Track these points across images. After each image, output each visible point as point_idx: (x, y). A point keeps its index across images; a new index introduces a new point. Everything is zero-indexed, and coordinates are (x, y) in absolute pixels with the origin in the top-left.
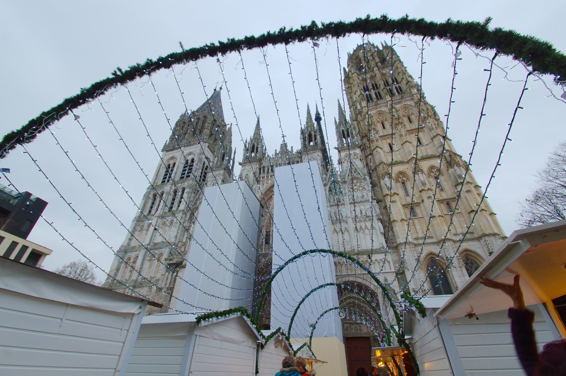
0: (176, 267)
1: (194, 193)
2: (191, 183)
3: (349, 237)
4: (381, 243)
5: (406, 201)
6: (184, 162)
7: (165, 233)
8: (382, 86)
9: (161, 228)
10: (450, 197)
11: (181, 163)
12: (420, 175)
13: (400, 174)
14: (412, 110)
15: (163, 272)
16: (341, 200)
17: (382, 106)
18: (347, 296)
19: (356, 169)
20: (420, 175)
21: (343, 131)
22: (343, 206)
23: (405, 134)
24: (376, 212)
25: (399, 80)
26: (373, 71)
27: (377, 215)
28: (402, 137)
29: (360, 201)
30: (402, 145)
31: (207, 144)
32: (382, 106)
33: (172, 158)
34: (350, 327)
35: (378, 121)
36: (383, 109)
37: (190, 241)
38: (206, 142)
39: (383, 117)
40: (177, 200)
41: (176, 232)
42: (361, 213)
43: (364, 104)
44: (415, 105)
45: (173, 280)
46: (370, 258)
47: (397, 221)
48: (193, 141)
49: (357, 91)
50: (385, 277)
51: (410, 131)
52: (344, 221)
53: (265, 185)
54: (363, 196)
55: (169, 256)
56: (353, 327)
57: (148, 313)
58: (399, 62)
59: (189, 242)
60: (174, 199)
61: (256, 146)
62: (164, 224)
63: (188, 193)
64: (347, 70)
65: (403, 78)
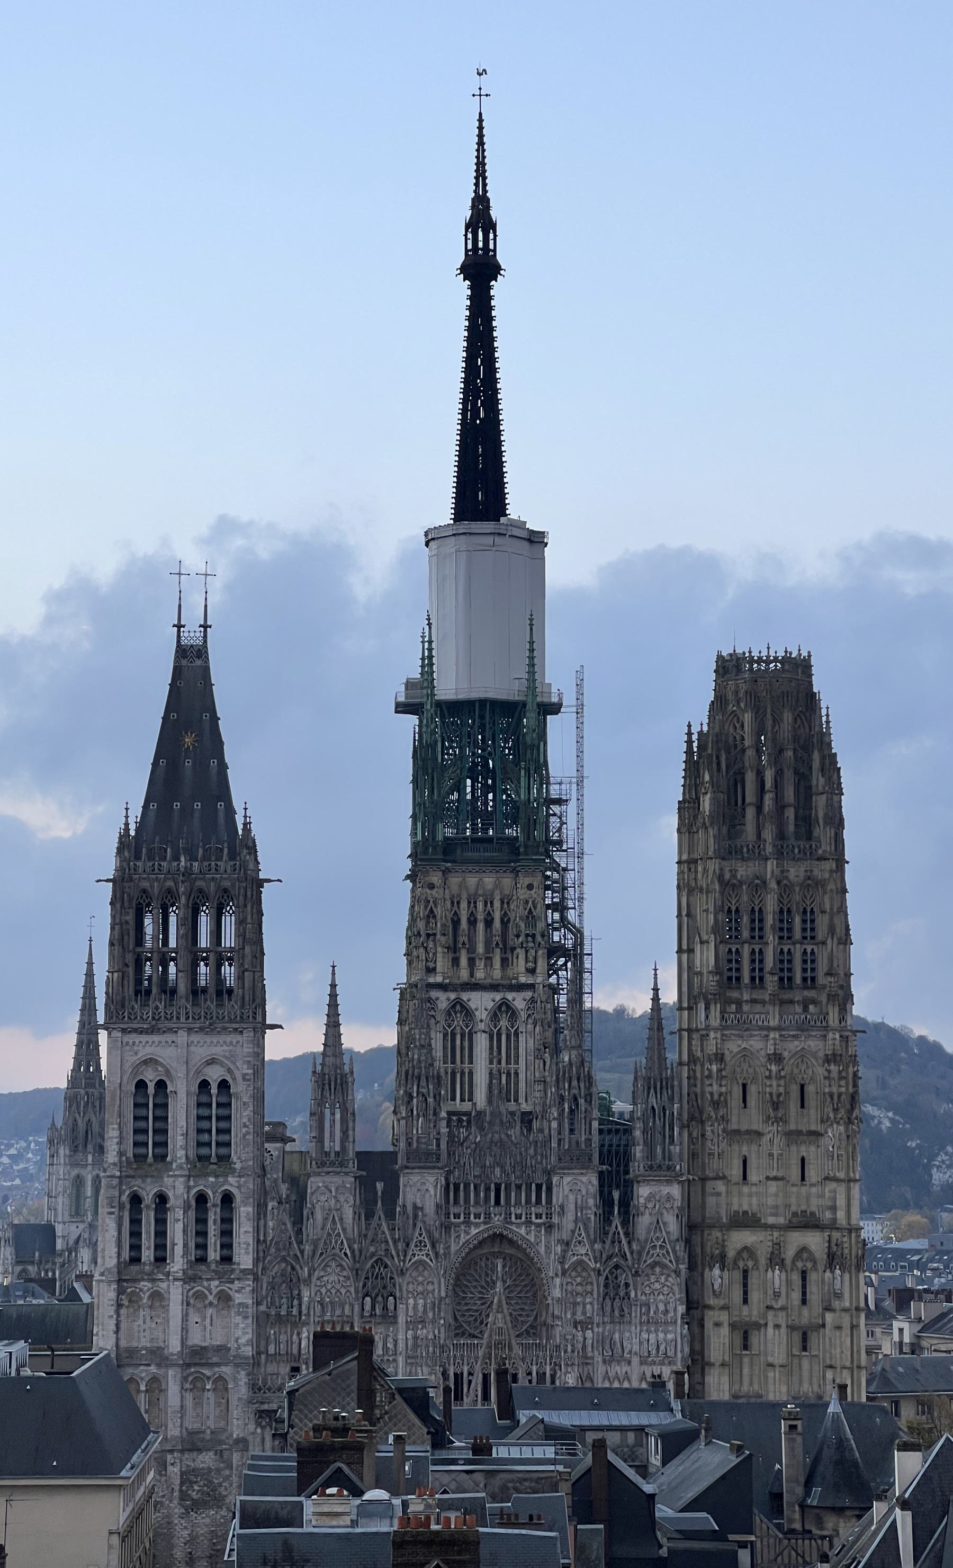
6: (195, 1088)
9: (194, 1306)
12: (777, 1272)
15: (251, 1427)
17: (755, 1035)
19: (664, 1242)
20: (777, 1272)
24: (682, 1351)
32: (755, 1035)
33: (149, 1062)
39: (750, 1066)
47: (713, 1365)
51: (793, 1136)
54: (666, 1312)
60: (201, 1221)
62: (199, 1296)
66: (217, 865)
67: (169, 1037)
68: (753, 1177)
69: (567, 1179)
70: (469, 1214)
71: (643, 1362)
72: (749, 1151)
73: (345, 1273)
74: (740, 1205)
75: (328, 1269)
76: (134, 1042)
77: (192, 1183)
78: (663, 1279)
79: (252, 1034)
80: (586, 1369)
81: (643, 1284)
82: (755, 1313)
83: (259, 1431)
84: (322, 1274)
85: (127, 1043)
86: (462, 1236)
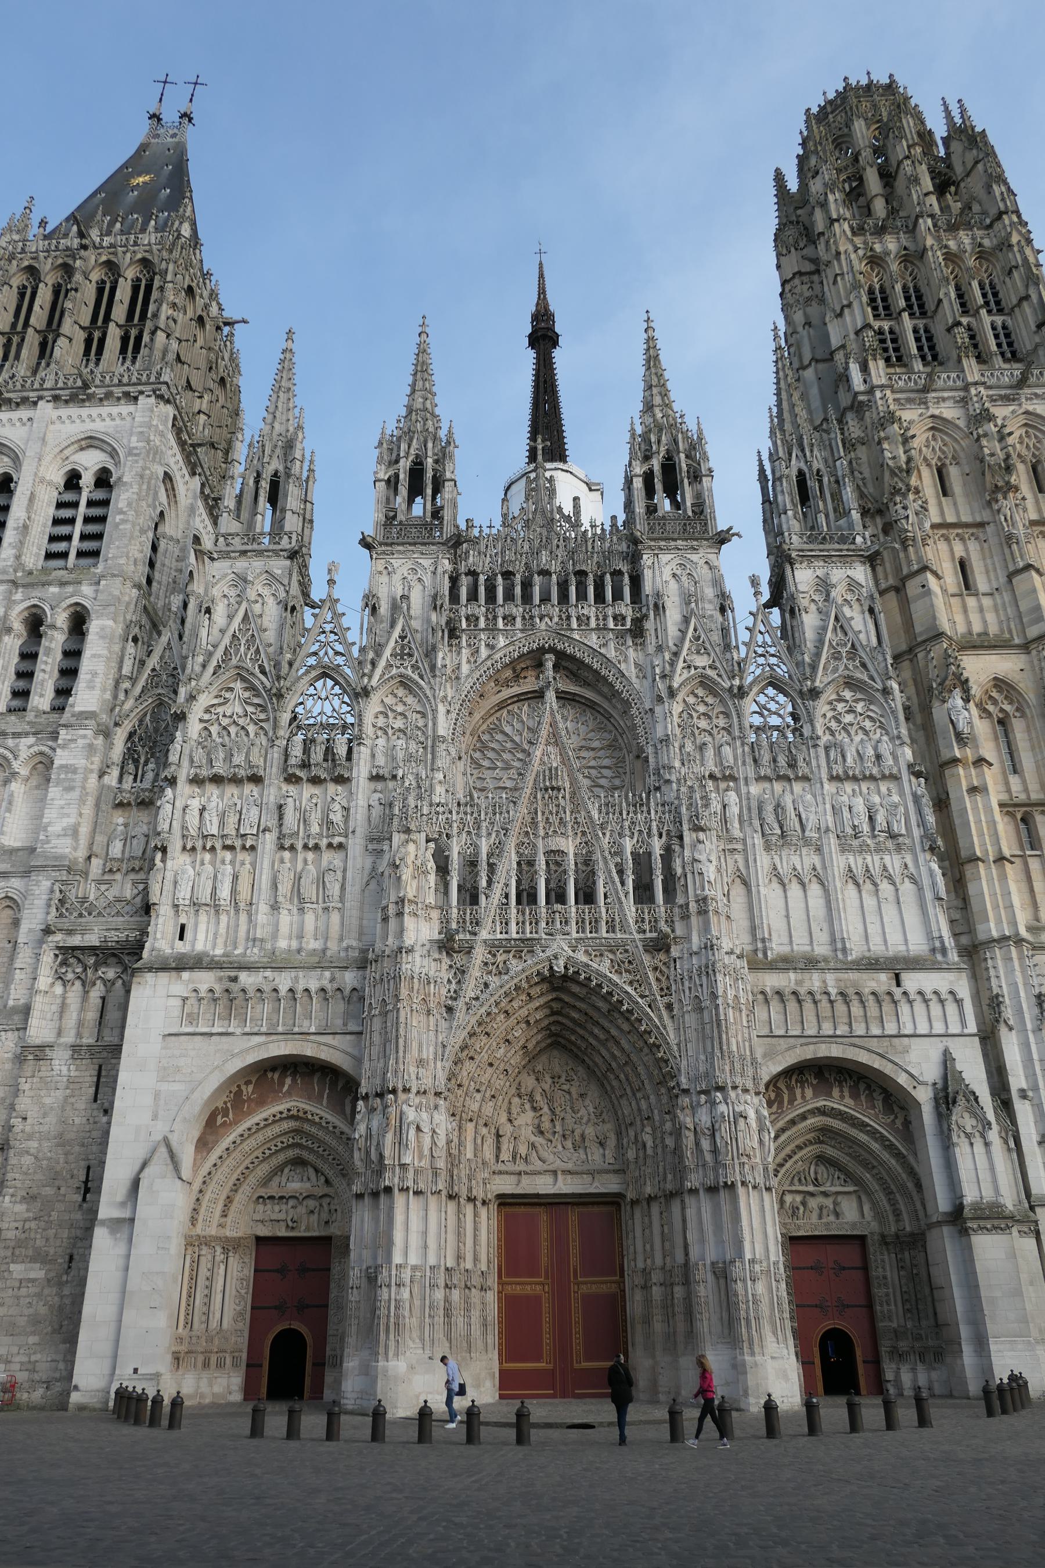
1: (135, 640)
2: (117, 593)
3: (821, 902)
5: (1009, 791)
7: (9, 810)
11: (42, 481)
13: (995, 686)
16: (801, 763)
17: (944, 399)
18: (809, 1107)
21: (801, 474)
22: (806, 785)
24: (922, 823)
25: (1009, 297)
26: (912, 229)
28: (1015, 547)
29: (868, 773)
30: (1010, 576)
31: (170, 410)
32: (944, 399)
34: (804, 1203)
35: (925, 459)
36: (949, 412)
37: (163, 861)
38: (168, 401)
40: (50, 661)
41: (73, 811)
42: (870, 818)
43: (879, 371)
45: (92, 1015)
46: (898, 985)
49: (849, 305)
52: (807, 842)
53: (484, 652)
54: (878, 757)
55: (61, 915)
56: (813, 1203)
58: (1015, 219)
60: (29, 656)
61: (429, 474)
64: (793, 184)
65: (1027, 297)
67: (24, 413)
68: (982, 583)
69: (665, 558)
70: (495, 618)
71: (844, 849)
72: (967, 550)
73: (256, 701)
74: (969, 623)
75: (227, 695)
77: (18, 596)
79: (152, 400)
80: (731, 862)
82: (1034, 786)
83: (58, 989)
84: (216, 701)
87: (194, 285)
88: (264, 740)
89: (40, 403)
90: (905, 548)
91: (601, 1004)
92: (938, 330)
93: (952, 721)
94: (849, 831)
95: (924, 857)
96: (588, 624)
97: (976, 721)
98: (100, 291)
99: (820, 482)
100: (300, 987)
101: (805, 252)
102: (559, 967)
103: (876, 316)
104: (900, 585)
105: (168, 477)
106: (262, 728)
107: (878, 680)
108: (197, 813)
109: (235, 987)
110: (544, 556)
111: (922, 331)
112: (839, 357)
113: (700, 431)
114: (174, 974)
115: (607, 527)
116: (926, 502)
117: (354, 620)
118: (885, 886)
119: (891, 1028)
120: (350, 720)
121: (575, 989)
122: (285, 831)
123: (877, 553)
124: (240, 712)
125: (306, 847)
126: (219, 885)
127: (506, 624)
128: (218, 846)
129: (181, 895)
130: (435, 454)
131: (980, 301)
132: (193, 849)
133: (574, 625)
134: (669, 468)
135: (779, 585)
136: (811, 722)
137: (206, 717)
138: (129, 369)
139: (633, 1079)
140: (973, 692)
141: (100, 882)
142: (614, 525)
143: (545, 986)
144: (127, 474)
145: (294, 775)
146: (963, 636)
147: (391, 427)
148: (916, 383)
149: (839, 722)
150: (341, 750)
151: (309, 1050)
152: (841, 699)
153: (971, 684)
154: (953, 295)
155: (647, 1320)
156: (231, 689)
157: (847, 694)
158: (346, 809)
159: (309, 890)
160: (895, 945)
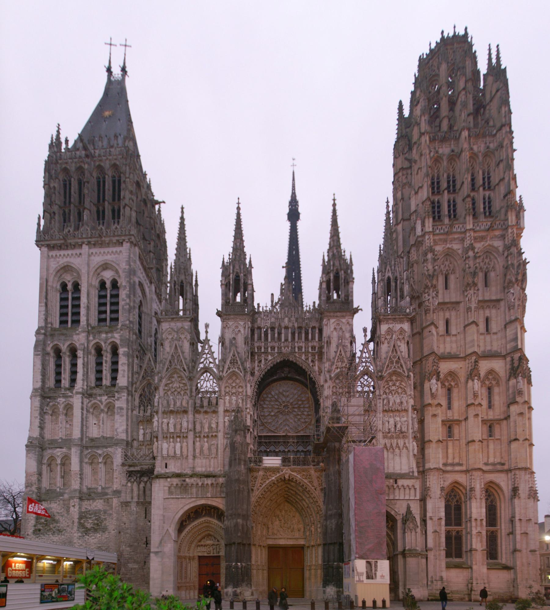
0: (140, 477)
4: (411, 467)
8: (466, 189)
10: (496, 417)
14: (495, 261)
20: (476, 381)
23: (475, 308)
24: (413, 428)
27: (414, 432)
30: (465, 327)
37: (157, 441)
42: (395, 426)
44: (504, 251)
46: (396, 483)
48: (107, 236)
50: (408, 505)
57: (116, 531)
59: (156, 443)
63: (128, 355)
66: (110, 151)
70: (267, 348)
71: (384, 437)
75: (173, 380)
76: (56, 256)
78: (398, 384)
79: (128, 244)
81: (384, 387)
84: (169, 382)
85: (52, 256)
86: (263, 361)
87: (139, 180)
88: (187, 398)
89: (84, 246)
90: (426, 314)
91: (300, 488)
92: (459, 201)
93: (431, 389)
94: (387, 431)
95: (411, 440)
96: (302, 350)
97: (440, 389)
98: (99, 183)
99: (396, 283)
100: (206, 483)
101: (407, 155)
102: (287, 477)
103: (433, 193)
104: (420, 331)
105: (141, 284)
106: (185, 392)
107: (406, 372)
108: (166, 424)
109: (184, 483)
110: (286, 320)
111: (452, 202)
112: (413, 217)
113: (351, 259)
114: (165, 479)
115: (312, 308)
116: (438, 292)
117: (216, 348)
118: (397, 450)
119: (391, 497)
120: (217, 389)
121: (293, 484)
122: (197, 431)
123: (414, 317)
124: (178, 386)
125: (204, 436)
126: (176, 450)
127: (271, 350)
128: (175, 436)
129: (163, 453)
130: (244, 272)
131: (481, 182)
132: (167, 437)
133: (297, 350)
134: (337, 277)
135: (374, 331)
136: (379, 389)
137: (166, 388)
138: (116, 228)
139: (309, 511)
140: (441, 377)
141: (137, 449)
142: (314, 306)
143: (282, 483)
144: (123, 282)
145: (198, 410)
146: (442, 354)
147: (226, 260)
148: (444, 230)
149: (389, 389)
150: (214, 401)
151: (209, 503)
152: (391, 380)
153: (440, 374)
154: (469, 179)
155: (310, 579)
156: (173, 377)
157: (394, 378)
158: (217, 423)
159: (206, 451)
160: (398, 470)
